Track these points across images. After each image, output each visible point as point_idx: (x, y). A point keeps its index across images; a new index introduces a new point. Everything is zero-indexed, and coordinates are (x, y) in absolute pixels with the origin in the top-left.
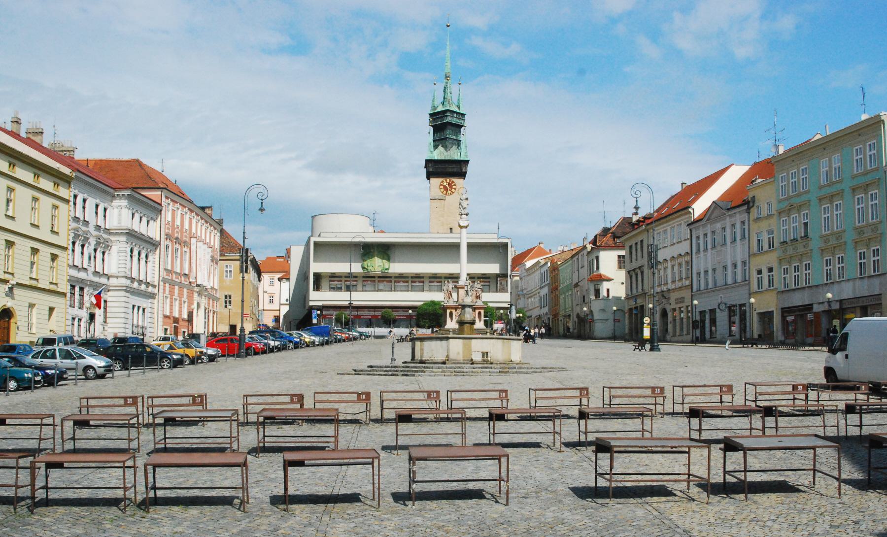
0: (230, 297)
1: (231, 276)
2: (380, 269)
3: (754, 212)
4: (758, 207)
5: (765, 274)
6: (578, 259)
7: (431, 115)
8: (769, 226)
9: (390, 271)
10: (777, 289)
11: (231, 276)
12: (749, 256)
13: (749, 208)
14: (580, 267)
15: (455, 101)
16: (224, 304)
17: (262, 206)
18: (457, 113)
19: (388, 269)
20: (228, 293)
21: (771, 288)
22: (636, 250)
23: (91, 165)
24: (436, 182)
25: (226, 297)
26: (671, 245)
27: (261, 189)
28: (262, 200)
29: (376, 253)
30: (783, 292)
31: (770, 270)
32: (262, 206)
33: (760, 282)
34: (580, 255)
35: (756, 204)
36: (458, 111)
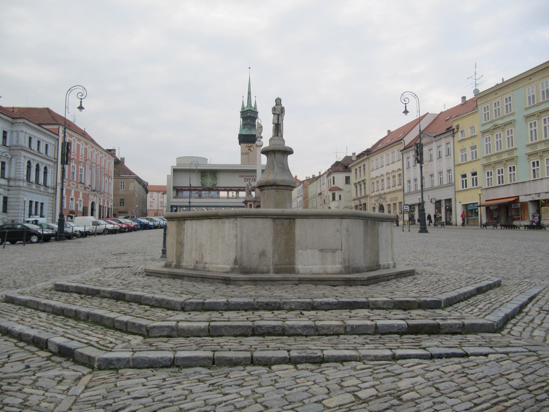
0: (123, 199)
1: (124, 188)
2: (211, 184)
3: (459, 136)
4: (462, 132)
5: (469, 178)
6: (320, 180)
7: (241, 112)
8: (473, 143)
9: (217, 186)
10: (481, 187)
11: (124, 188)
12: (455, 166)
13: (454, 133)
14: (322, 184)
15: (253, 105)
16: (119, 204)
17: (81, 104)
18: (254, 111)
19: (216, 185)
20: (122, 198)
21: (475, 187)
22: (360, 171)
23: (16, 111)
24: (244, 145)
25: (121, 199)
26: (392, 163)
27: (80, 90)
28: (81, 99)
29: (209, 175)
30: (487, 189)
31: (474, 174)
32: (81, 104)
33: (464, 184)
34: (322, 178)
35: (460, 130)
36: (254, 110)
